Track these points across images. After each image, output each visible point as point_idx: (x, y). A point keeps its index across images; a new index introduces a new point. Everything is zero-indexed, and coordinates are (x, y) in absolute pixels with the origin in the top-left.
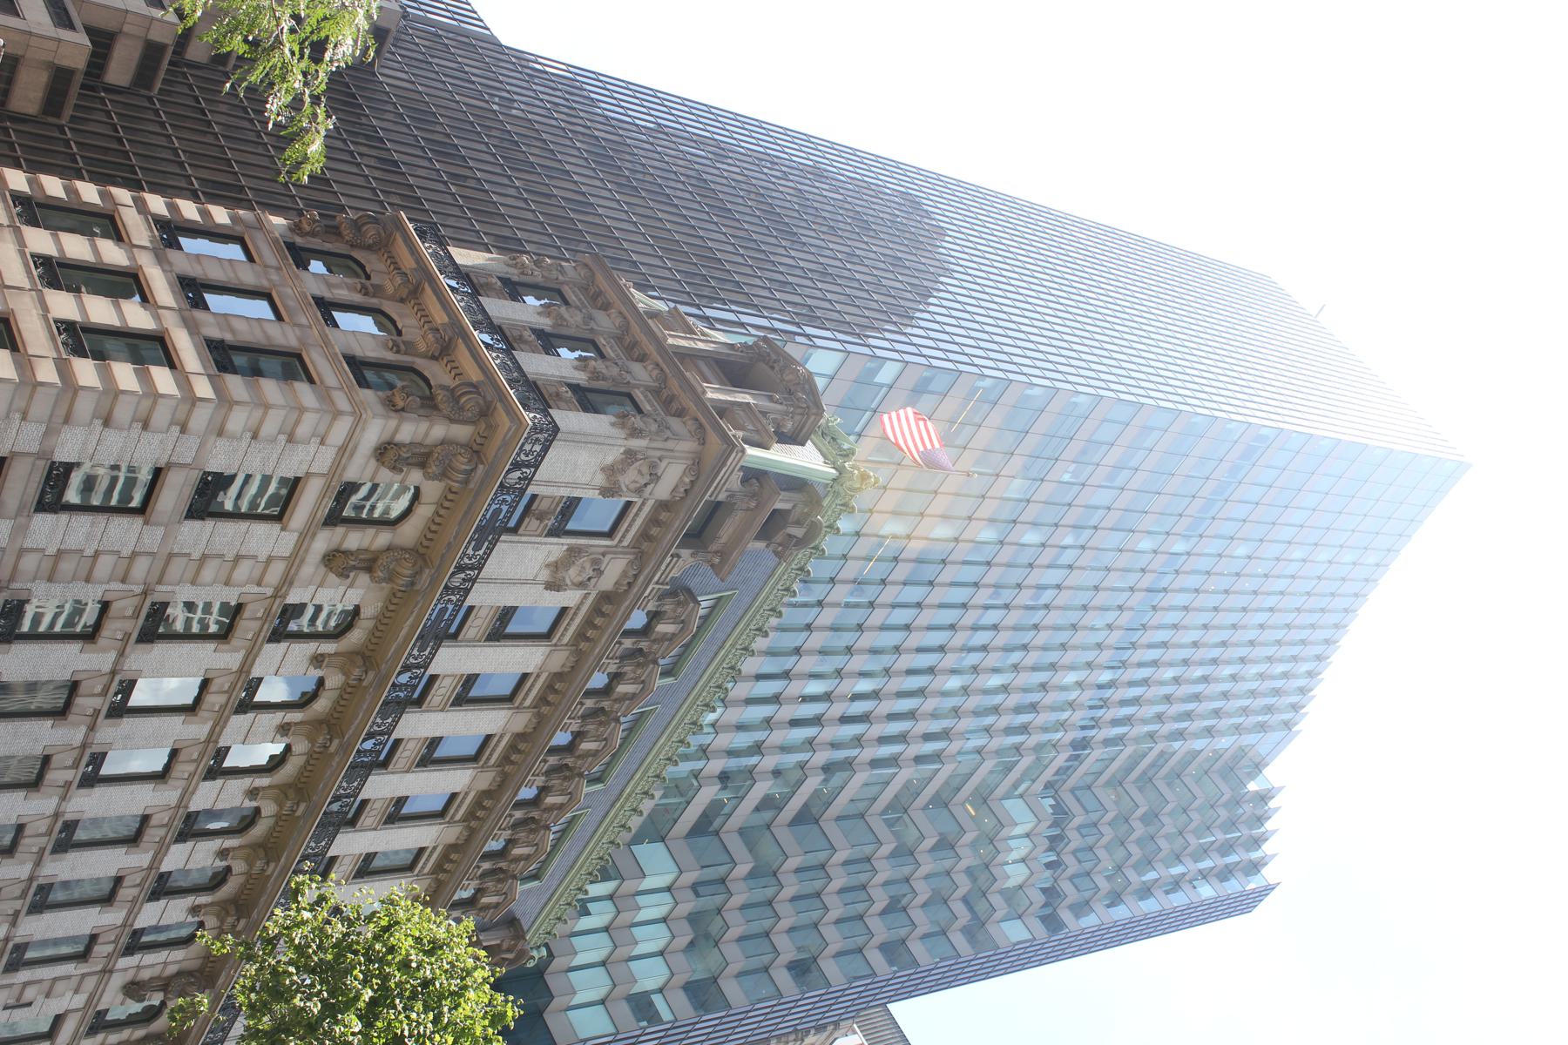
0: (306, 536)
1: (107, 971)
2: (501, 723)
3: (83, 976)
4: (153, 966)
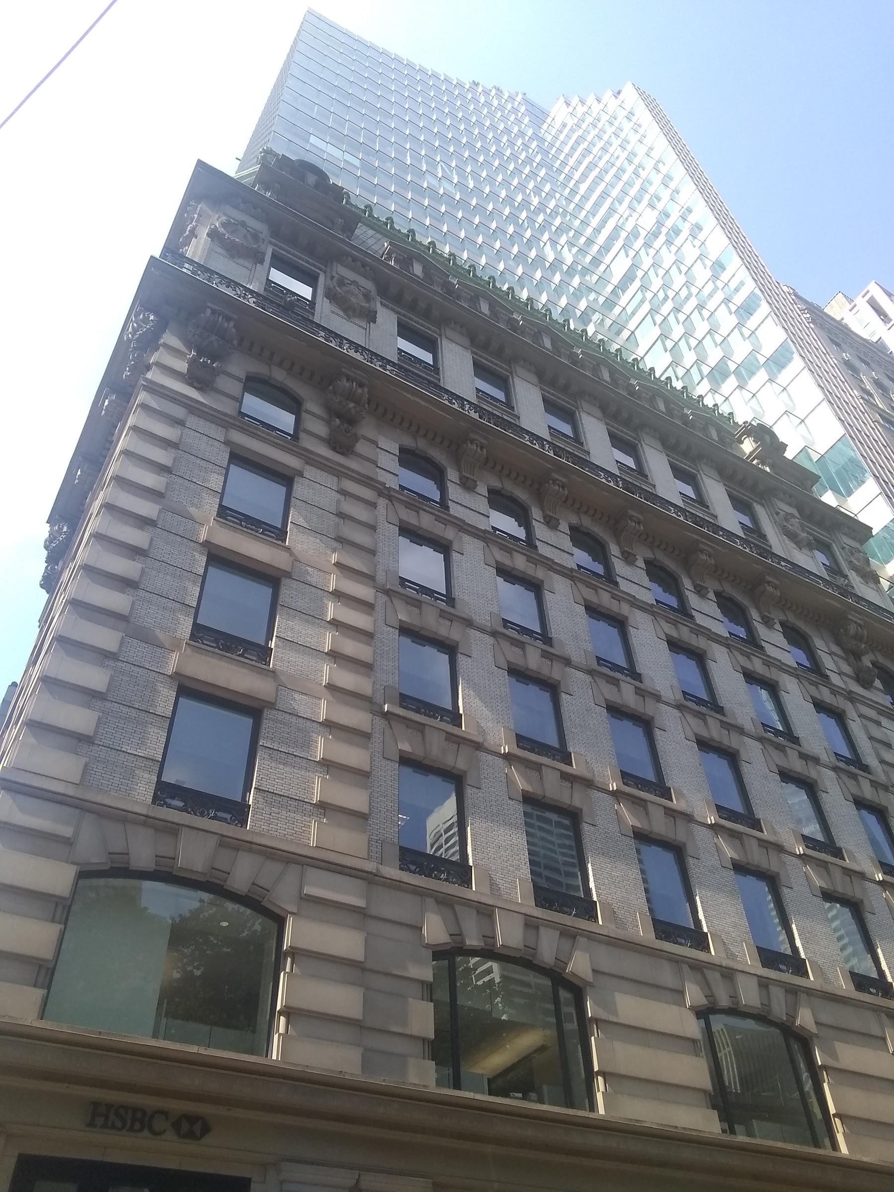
0: (311, 459)
1: (851, 697)
2: (530, 386)
3: (861, 716)
4: (835, 663)
